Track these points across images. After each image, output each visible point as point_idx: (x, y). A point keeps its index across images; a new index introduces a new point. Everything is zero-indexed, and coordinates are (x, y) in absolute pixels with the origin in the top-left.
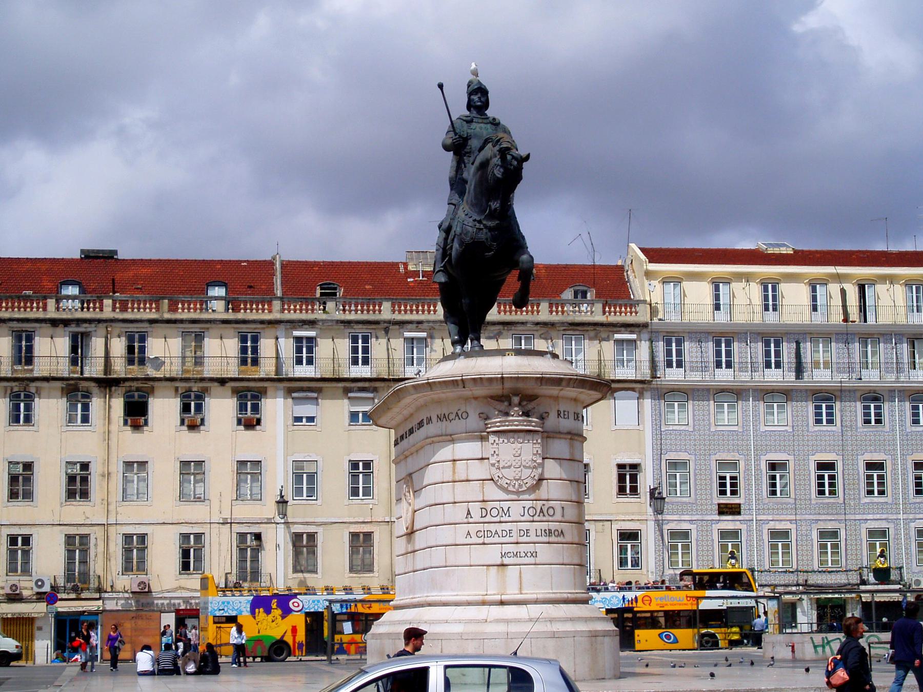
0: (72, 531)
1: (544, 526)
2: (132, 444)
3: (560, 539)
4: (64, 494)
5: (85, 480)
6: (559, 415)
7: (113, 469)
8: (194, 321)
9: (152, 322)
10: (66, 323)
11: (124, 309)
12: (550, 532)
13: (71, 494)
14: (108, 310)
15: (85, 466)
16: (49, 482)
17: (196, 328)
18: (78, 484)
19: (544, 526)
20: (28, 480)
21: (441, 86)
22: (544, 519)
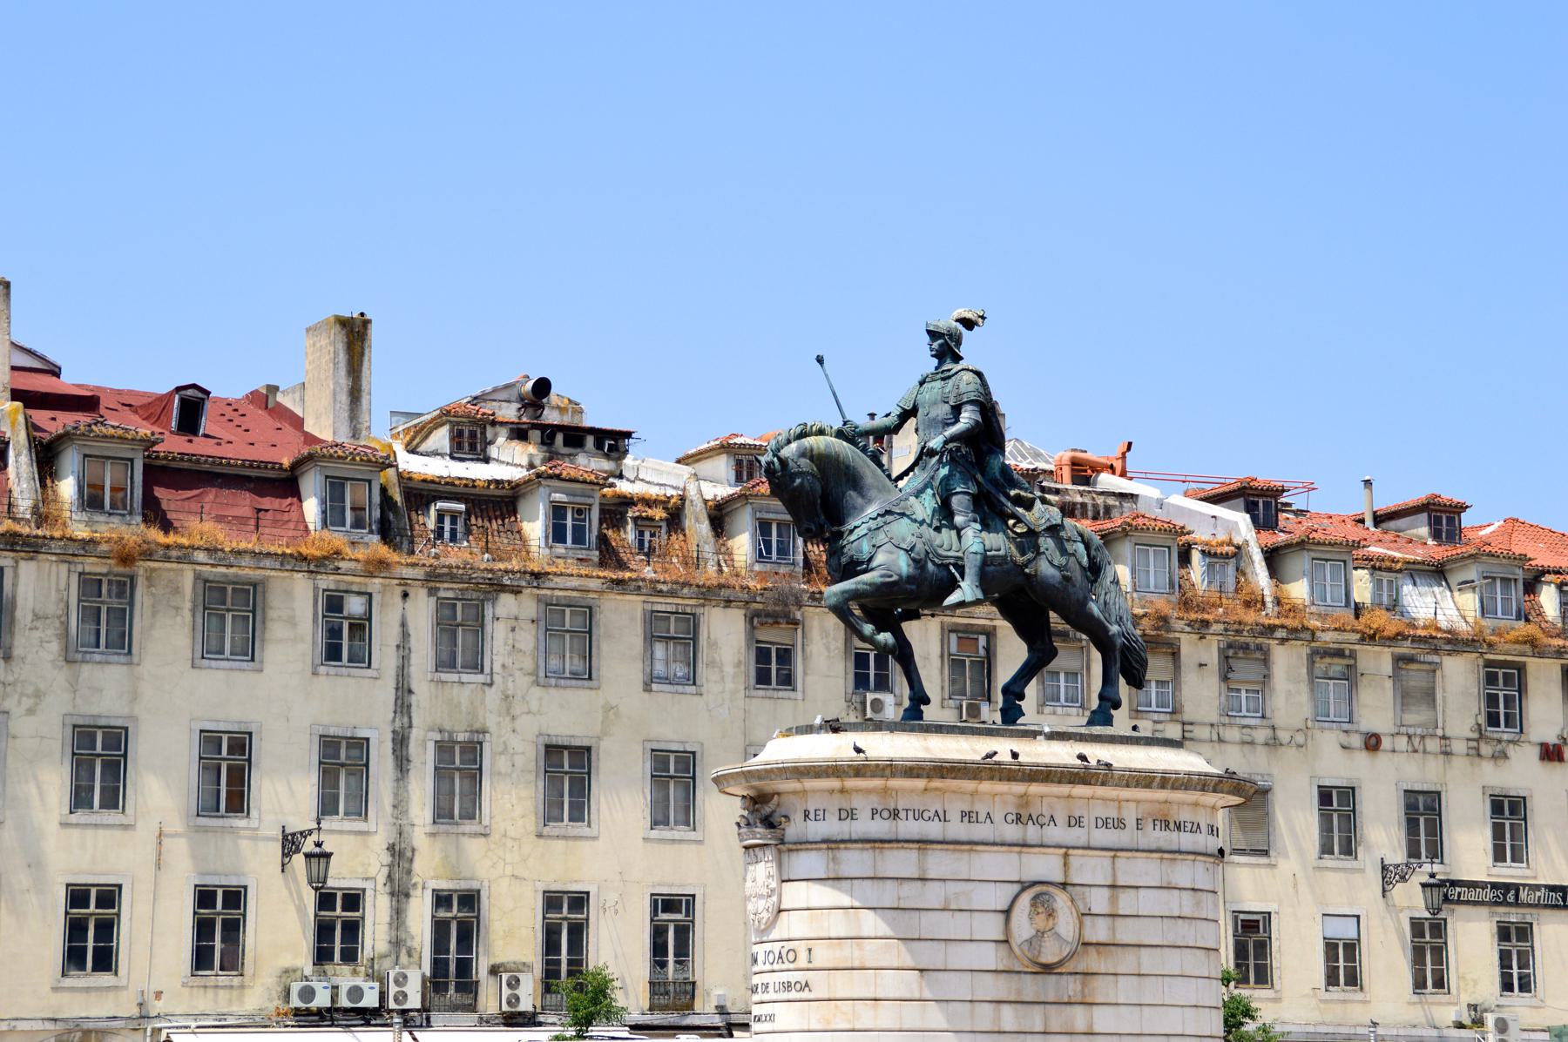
1: (785, 977)
3: (805, 995)
6: (806, 816)
12: (788, 986)
19: (785, 977)
21: (820, 360)
22: (784, 967)
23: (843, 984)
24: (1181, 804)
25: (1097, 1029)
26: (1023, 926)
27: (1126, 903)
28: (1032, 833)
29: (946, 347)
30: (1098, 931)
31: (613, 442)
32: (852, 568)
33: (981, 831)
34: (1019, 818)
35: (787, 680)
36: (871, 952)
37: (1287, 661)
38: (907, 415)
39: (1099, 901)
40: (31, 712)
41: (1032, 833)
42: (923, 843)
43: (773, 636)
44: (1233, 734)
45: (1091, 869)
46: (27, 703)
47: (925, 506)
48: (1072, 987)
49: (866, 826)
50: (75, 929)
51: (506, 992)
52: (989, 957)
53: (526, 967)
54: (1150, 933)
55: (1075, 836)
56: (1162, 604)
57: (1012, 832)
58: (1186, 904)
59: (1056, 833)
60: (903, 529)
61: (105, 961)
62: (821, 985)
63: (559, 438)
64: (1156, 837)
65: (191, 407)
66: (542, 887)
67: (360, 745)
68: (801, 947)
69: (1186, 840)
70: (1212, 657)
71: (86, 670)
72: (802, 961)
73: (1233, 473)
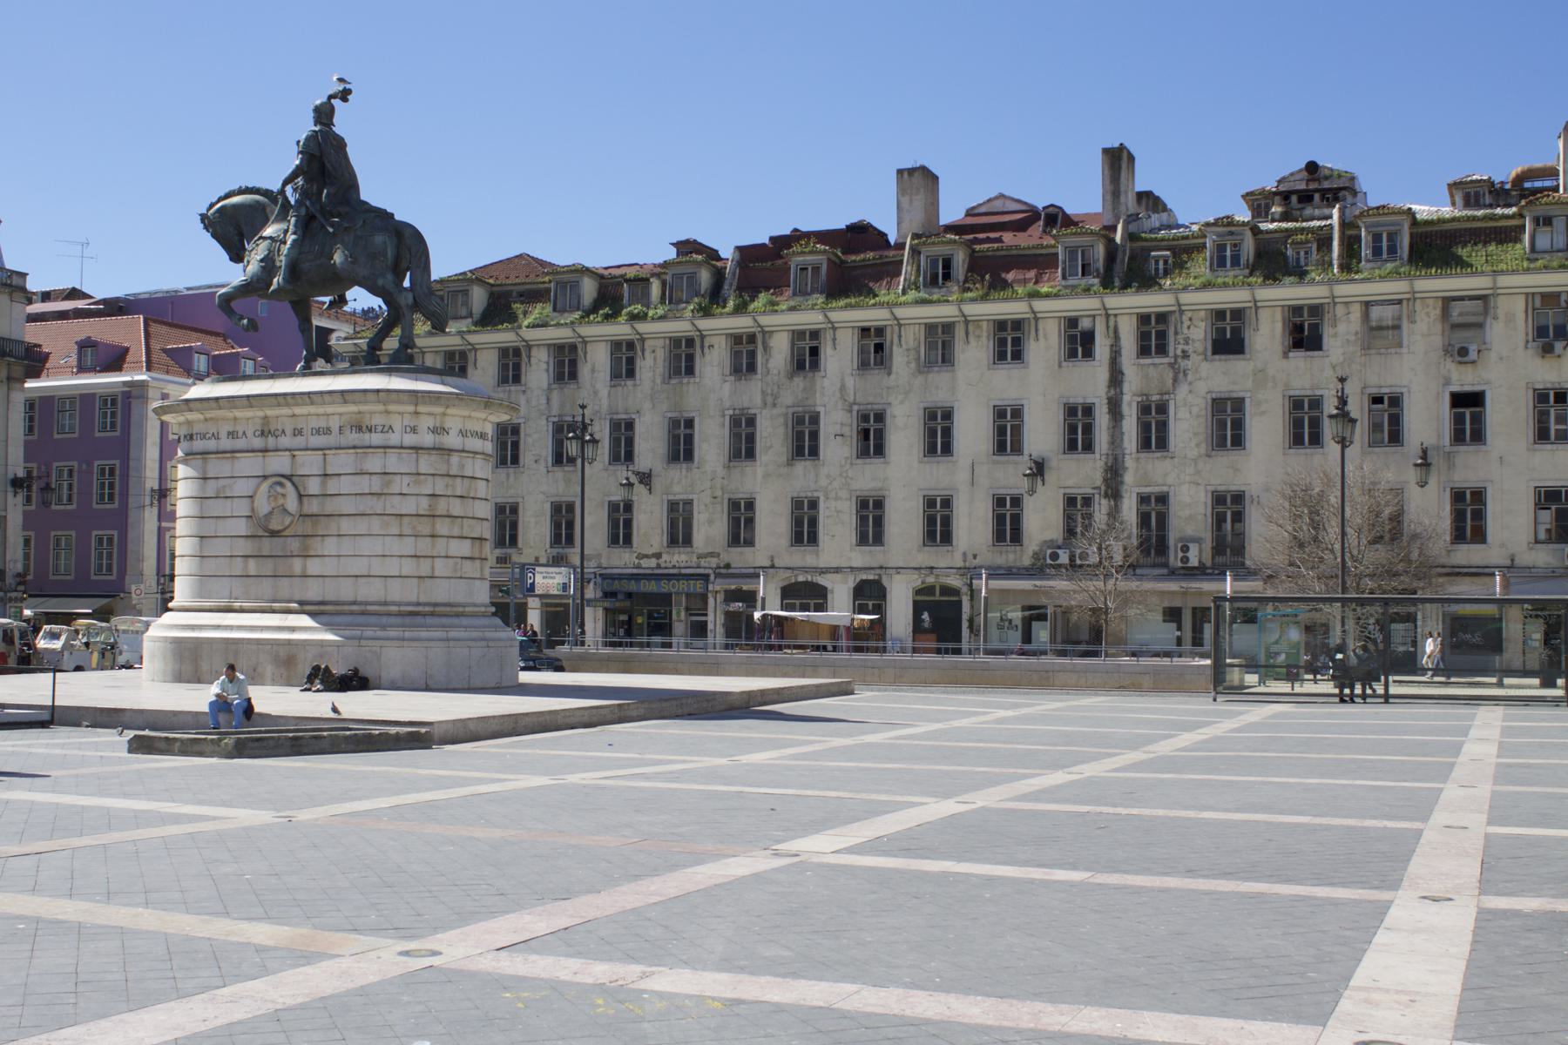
24: (372, 413)
25: (309, 572)
27: (333, 486)
28: (271, 442)
30: (313, 507)
33: (240, 443)
34: (263, 433)
39: (313, 487)
40: (902, 402)
41: (271, 442)
46: (900, 397)
50: (930, 521)
51: (1180, 555)
52: (242, 527)
53: (1198, 540)
54: (347, 506)
55: (299, 441)
57: (258, 443)
58: (376, 484)
59: (285, 441)
61: (947, 538)
63: (1294, 199)
64: (353, 437)
66: (1211, 488)
67: (1088, 410)
69: (376, 438)
71: (930, 376)
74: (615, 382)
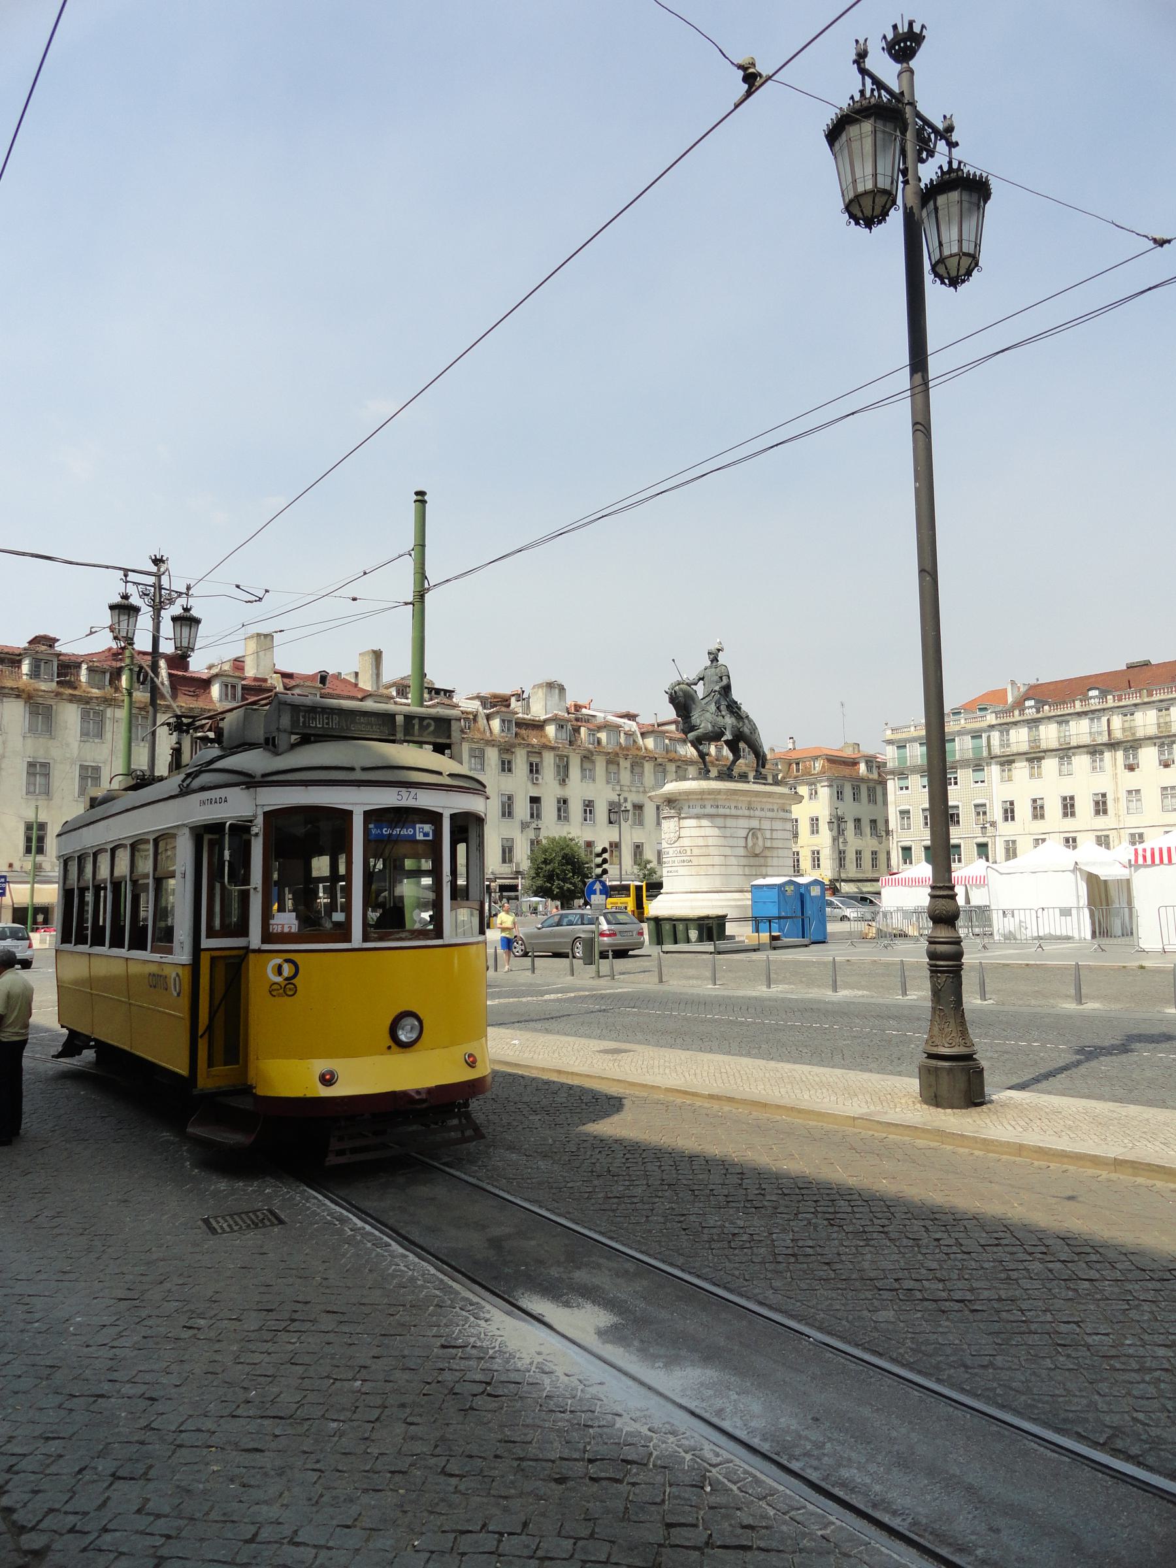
0: (1099, 833)
2: (1131, 780)
4: (1093, 812)
5: (1104, 803)
7: (1119, 795)
8: (1161, 701)
9: (1135, 705)
10: (1085, 713)
11: (1120, 700)
13: (1097, 812)
14: (1110, 702)
15: (1104, 795)
16: (1084, 806)
17: (1164, 705)
18: (1101, 807)
20: (1072, 806)
23: (703, 860)
26: (750, 844)
29: (715, 659)
30: (768, 844)
31: (449, 693)
32: (693, 728)
33: (739, 812)
35: (510, 770)
36: (712, 851)
37: (648, 767)
38: (702, 679)
42: (725, 816)
43: (506, 757)
44: (634, 789)
45: (766, 825)
47: (713, 707)
48: (762, 861)
49: (709, 810)
52: (742, 852)
55: (762, 814)
56: (617, 749)
57: (747, 813)
59: (758, 813)
60: (708, 715)
62: (695, 861)
65: (323, 678)
68: (688, 849)
70: (629, 766)
72: (689, 853)
73: (624, 710)
74: (85, 738)
